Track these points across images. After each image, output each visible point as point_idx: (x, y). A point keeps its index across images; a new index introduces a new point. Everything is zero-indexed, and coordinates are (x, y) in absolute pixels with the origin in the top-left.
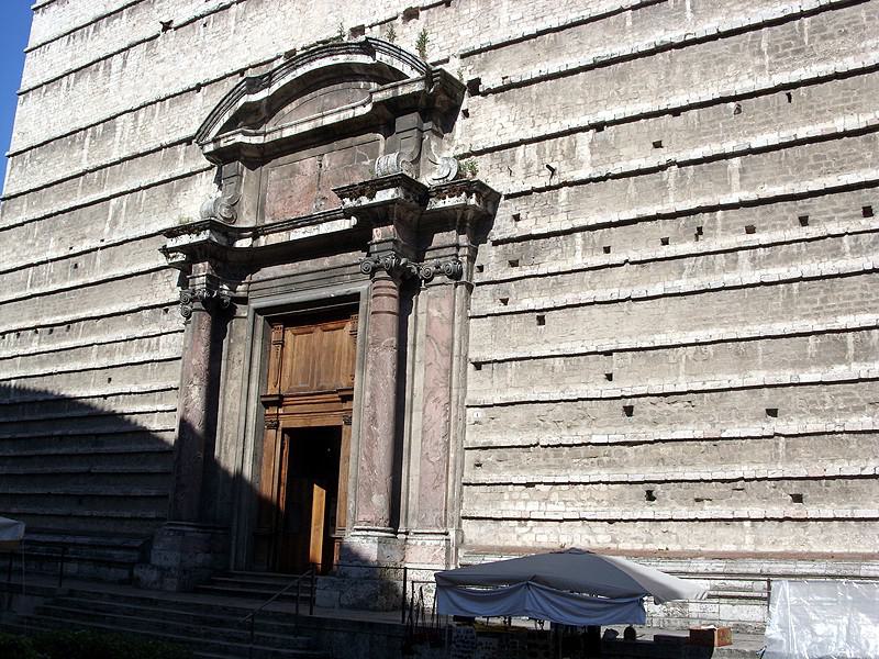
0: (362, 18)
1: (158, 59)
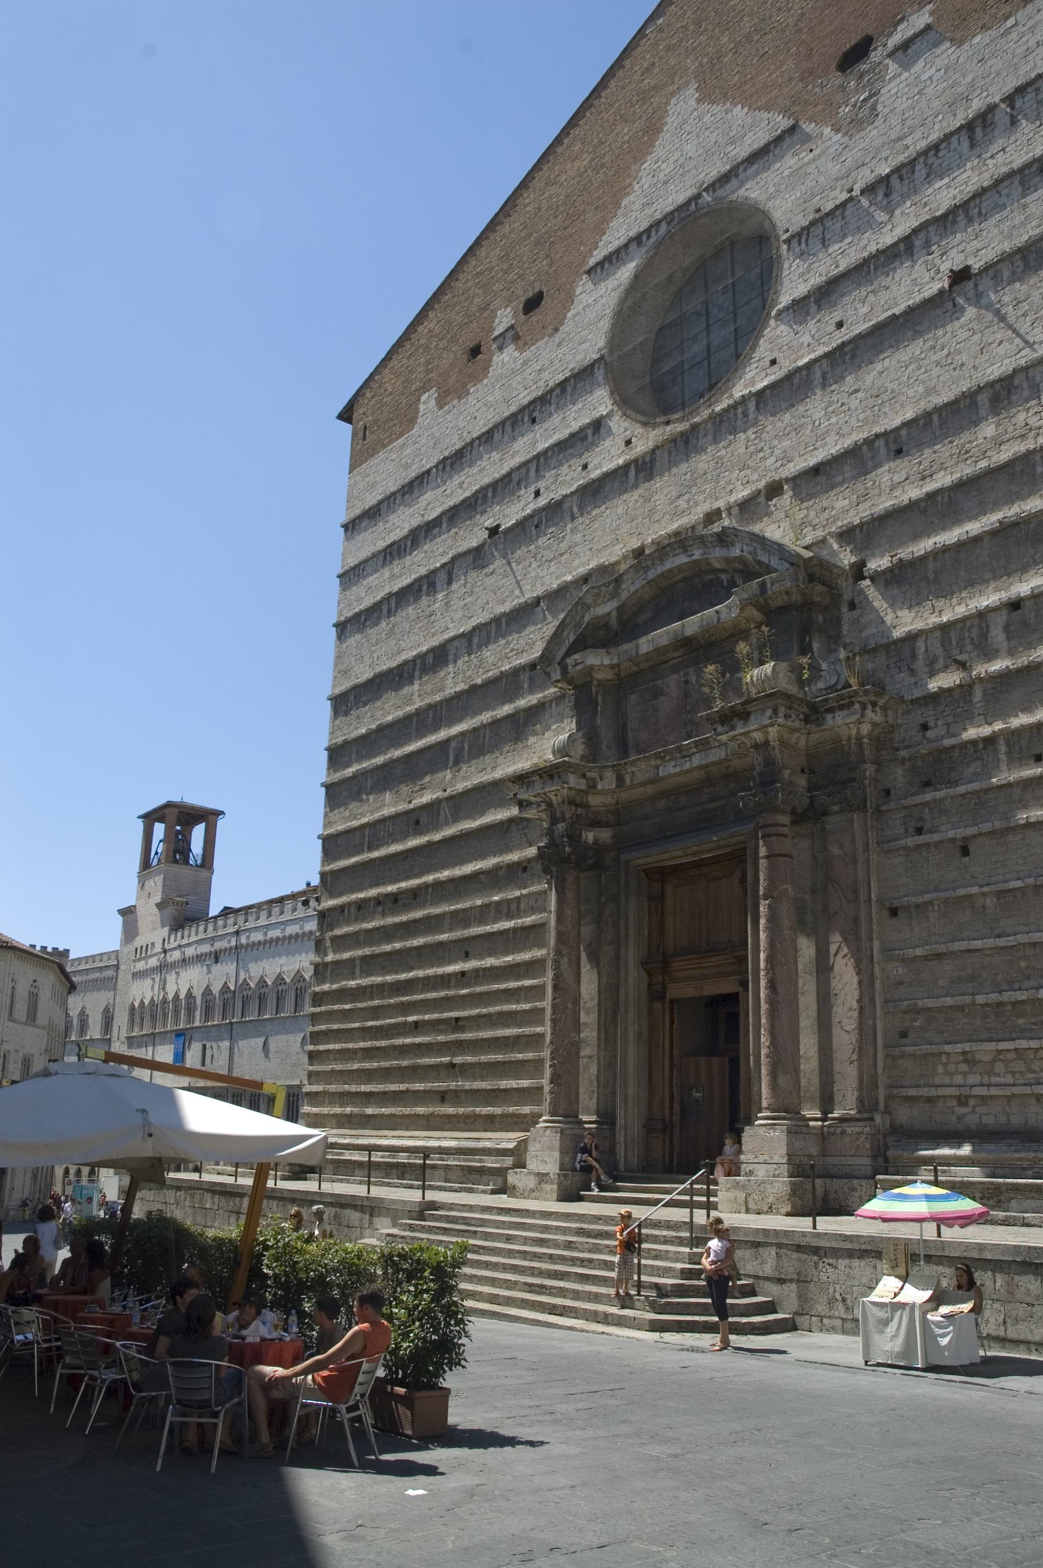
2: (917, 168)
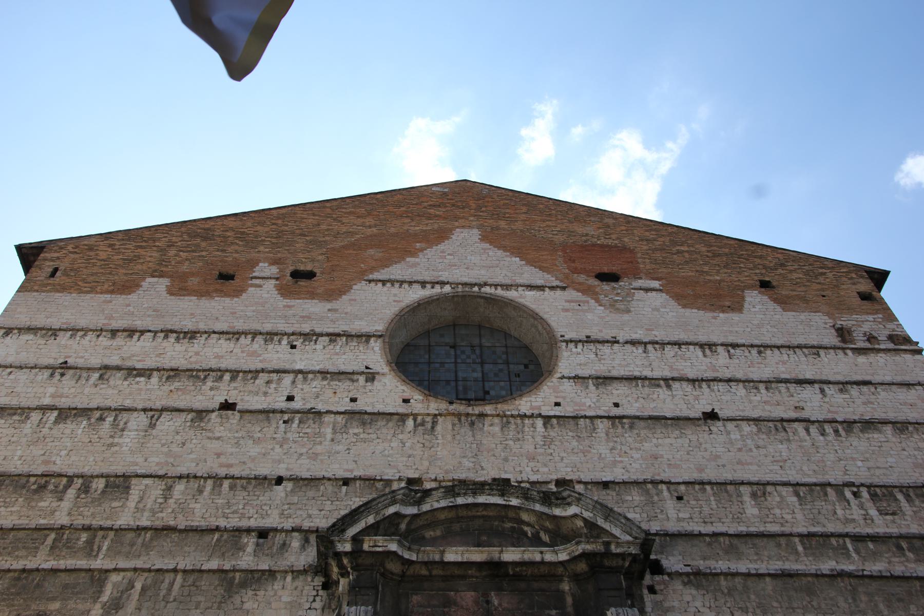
0: (506, 472)
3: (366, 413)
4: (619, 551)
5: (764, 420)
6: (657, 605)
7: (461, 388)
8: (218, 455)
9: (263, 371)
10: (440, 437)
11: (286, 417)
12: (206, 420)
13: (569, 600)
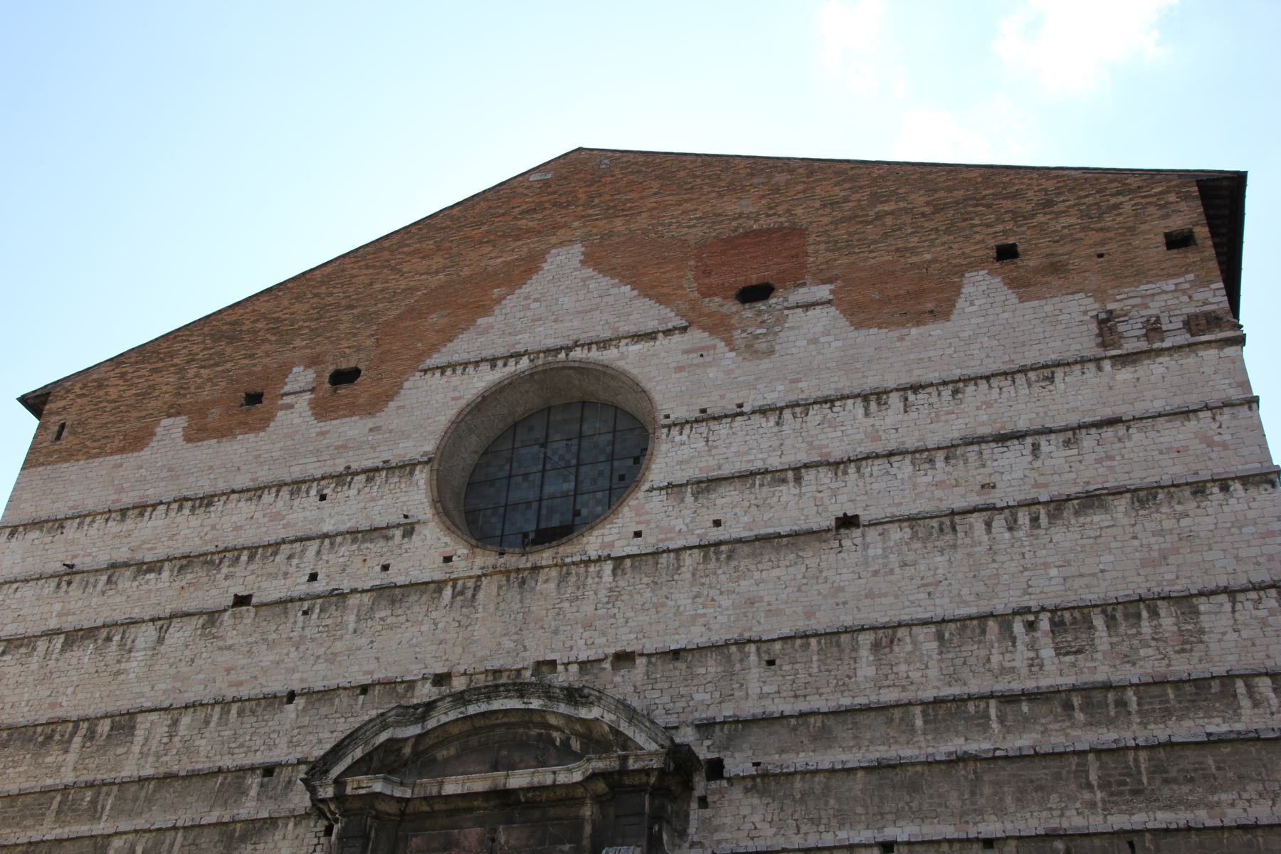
0: (553, 651)
1: (221, 643)
2: (811, 412)
3: (396, 586)
4: (637, 766)
5: (925, 518)
6: (705, 822)
7: (544, 511)
8: (228, 671)
9: (284, 541)
10: (481, 609)
11: (306, 606)
12: (217, 624)
13: (588, 829)
